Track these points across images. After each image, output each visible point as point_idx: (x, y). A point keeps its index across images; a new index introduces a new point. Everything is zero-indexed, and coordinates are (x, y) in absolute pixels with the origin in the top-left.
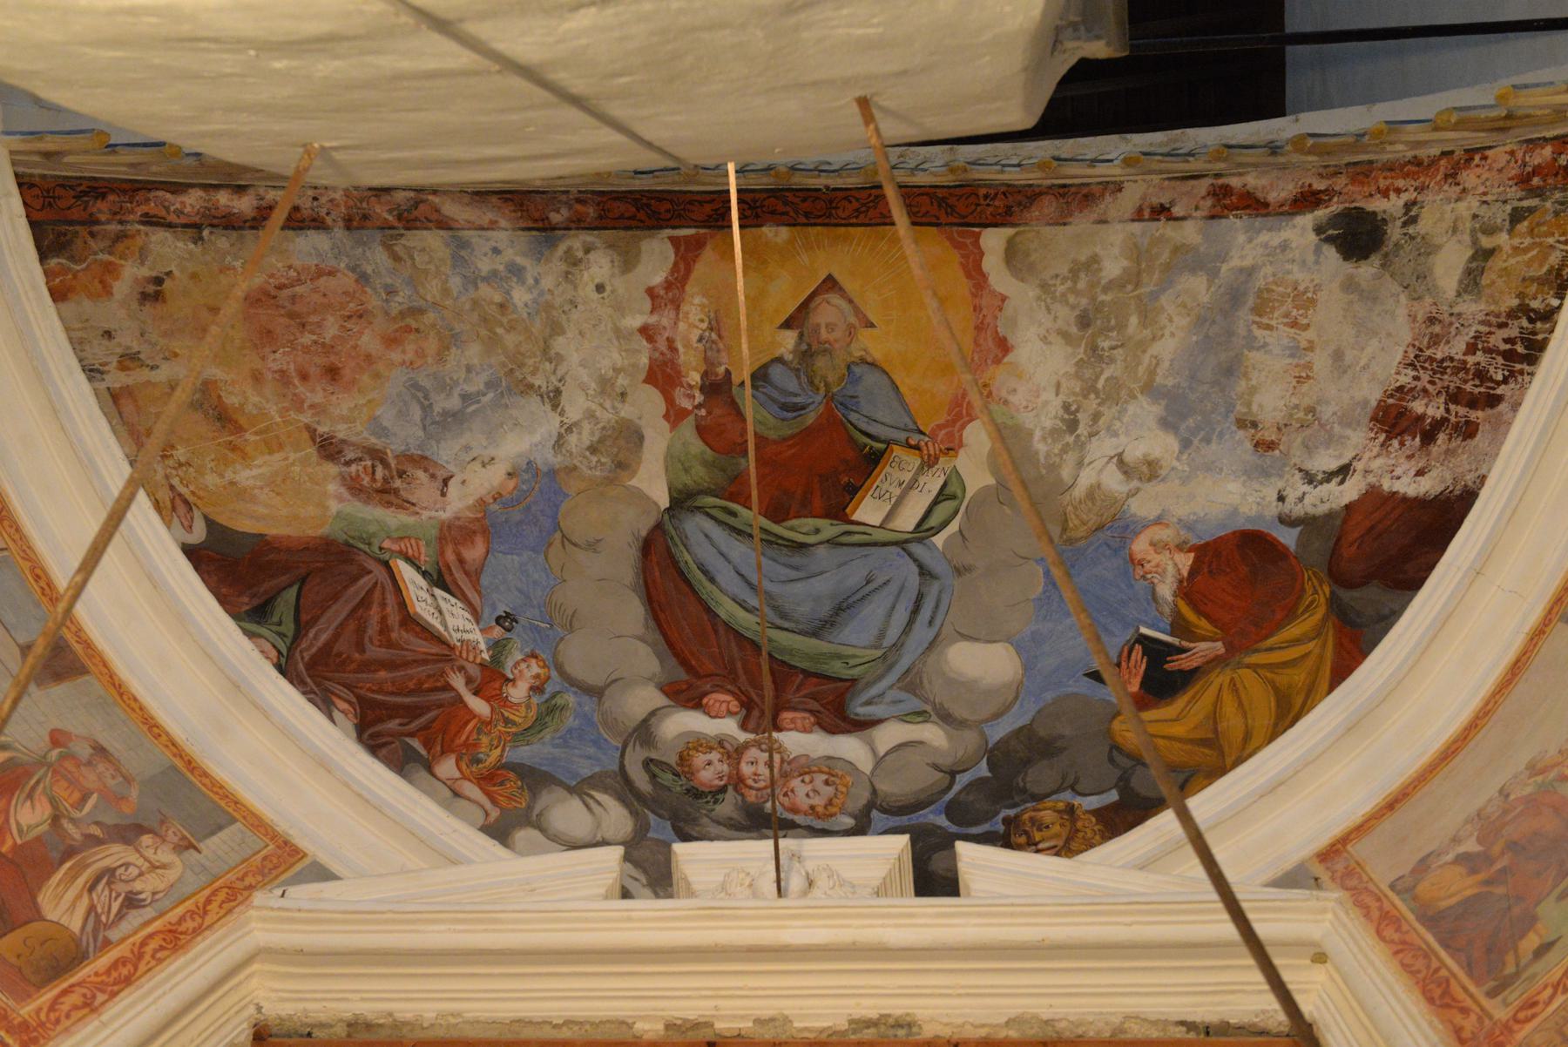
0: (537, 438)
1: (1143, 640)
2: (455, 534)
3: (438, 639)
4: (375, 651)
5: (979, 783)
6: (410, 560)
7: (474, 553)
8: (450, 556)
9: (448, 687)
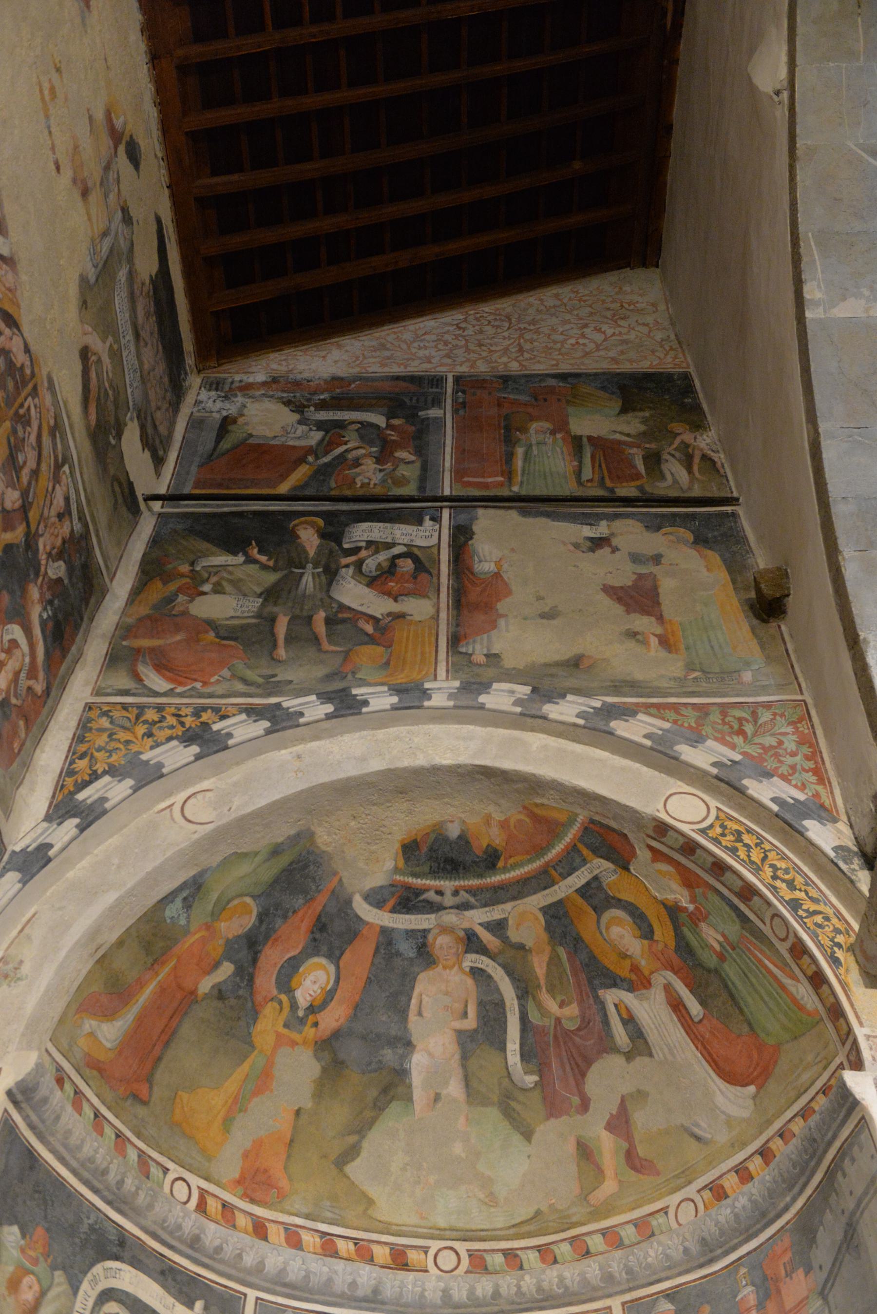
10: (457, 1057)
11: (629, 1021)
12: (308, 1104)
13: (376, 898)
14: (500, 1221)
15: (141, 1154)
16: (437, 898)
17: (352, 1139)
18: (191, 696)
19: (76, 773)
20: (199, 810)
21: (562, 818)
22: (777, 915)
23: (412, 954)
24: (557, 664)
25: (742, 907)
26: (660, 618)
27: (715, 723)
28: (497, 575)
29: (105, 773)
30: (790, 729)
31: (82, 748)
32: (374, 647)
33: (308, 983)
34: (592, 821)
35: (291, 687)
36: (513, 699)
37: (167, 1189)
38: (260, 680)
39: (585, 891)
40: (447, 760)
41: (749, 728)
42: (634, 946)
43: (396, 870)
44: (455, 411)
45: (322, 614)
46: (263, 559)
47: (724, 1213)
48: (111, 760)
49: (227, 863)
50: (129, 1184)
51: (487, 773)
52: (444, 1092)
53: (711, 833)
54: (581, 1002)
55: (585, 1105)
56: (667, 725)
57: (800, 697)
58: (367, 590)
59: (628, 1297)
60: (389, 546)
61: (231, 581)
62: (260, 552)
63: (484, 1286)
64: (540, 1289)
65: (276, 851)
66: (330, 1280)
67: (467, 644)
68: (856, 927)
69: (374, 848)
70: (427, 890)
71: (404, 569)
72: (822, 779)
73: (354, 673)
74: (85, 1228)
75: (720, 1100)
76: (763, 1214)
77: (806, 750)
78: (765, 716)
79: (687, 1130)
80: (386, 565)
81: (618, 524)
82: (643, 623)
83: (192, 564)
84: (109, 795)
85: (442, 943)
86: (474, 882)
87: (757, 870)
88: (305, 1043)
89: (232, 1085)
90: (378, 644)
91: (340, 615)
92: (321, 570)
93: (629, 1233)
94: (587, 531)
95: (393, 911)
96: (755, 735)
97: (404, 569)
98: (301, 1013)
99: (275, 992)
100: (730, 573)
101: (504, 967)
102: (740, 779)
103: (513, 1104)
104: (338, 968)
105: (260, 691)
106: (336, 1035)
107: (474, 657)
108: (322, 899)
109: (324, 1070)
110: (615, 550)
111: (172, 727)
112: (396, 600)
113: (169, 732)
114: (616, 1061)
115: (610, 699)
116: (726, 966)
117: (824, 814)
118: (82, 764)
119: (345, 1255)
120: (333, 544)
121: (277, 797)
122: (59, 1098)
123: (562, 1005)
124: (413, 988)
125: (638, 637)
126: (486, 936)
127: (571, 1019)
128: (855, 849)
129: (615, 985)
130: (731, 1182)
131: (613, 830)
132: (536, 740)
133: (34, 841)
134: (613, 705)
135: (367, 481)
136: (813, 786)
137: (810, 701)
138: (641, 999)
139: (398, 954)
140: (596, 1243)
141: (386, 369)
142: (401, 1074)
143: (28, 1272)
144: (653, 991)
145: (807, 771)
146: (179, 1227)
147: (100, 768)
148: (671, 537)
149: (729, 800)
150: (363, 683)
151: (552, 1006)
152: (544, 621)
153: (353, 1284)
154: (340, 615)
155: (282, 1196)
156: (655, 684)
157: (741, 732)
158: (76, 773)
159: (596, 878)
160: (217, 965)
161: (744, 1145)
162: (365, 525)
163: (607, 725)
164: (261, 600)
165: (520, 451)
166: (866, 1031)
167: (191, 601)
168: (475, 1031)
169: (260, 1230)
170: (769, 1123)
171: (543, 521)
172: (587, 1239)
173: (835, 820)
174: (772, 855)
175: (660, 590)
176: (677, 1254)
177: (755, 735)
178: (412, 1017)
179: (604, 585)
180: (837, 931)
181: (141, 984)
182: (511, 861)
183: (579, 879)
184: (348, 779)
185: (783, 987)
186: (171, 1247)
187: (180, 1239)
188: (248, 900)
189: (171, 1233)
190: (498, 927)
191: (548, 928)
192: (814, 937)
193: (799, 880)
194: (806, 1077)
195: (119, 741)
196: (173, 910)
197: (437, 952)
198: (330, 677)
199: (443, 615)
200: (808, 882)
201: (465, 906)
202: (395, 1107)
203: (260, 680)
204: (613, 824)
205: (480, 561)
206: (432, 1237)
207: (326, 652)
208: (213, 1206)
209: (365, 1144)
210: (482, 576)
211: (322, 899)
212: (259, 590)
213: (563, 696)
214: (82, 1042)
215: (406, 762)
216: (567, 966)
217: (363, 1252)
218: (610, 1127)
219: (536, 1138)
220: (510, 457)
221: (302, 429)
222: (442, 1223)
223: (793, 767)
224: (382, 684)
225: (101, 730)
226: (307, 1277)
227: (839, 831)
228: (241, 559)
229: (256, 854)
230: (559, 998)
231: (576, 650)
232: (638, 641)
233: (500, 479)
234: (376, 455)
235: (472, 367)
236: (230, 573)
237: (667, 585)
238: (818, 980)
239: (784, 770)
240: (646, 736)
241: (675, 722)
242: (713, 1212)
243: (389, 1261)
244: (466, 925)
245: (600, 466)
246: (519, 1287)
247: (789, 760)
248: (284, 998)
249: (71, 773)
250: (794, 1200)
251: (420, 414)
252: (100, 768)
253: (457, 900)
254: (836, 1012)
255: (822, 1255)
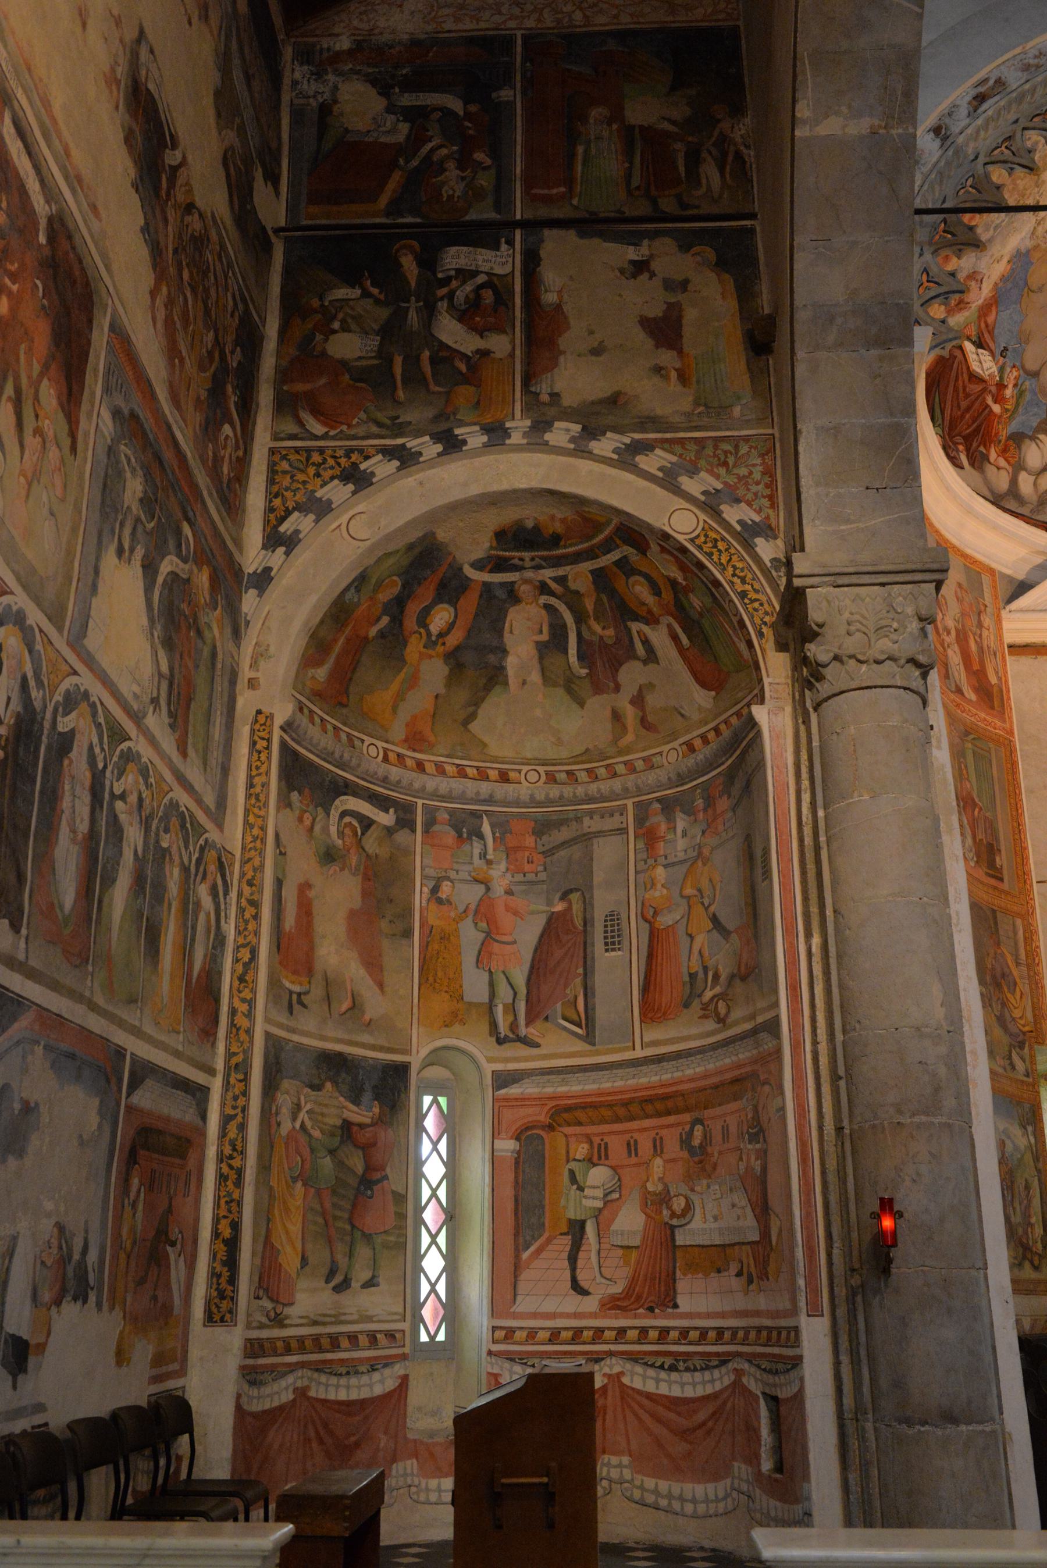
0: (1024, 234)
2: (984, 310)
3: (981, 380)
4: (964, 404)
6: (969, 338)
7: (990, 319)
8: (983, 325)
9: (987, 406)
10: (537, 657)
11: (646, 642)
12: (442, 691)
13: (479, 565)
14: (564, 754)
15: (348, 735)
16: (521, 563)
17: (471, 709)
18: (341, 439)
19: (275, 510)
20: (359, 529)
21: (602, 520)
22: (731, 601)
23: (504, 597)
24: (601, 402)
25: (713, 590)
26: (680, 352)
27: (709, 456)
28: (558, 307)
29: (294, 509)
30: (759, 461)
31: (275, 488)
32: (467, 387)
33: (437, 620)
34: (621, 524)
35: (411, 427)
36: (568, 437)
37: (365, 752)
38: (388, 422)
39: (618, 563)
40: (523, 486)
41: (731, 460)
42: (650, 599)
43: (491, 548)
44: (524, 93)
45: (426, 354)
46: (375, 291)
47: (691, 762)
48: (296, 498)
49: (379, 560)
50: (346, 756)
51: (552, 492)
52: (528, 679)
53: (697, 542)
54: (615, 628)
55: (617, 688)
56: (674, 459)
57: (770, 431)
58: (459, 326)
59: (637, 799)
60: (474, 274)
61: (353, 317)
62: (372, 285)
63: (554, 792)
64: (586, 795)
65: (410, 547)
66: (464, 792)
67: (536, 383)
68: (778, 608)
69: (476, 536)
70: (513, 558)
71: (487, 301)
72: (774, 505)
73: (455, 414)
74: (327, 783)
75: (696, 695)
76: (711, 765)
77: (767, 479)
78: (744, 449)
79: (676, 709)
80: (472, 296)
81: (657, 243)
82: (667, 358)
83: (321, 298)
84: (300, 528)
85: (524, 589)
86: (545, 553)
87: (723, 569)
88: (438, 656)
89: (395, 687)
90: (470, 384)
91: (441, 354)
92: (421, 304)
93: (640, 765)
94: (632, 253)
95: (491, 571)
96: (734, 466)
97: (487, 301)
98: (434, 638)
99: (416, 628)
100: (739, 302)
101: (566, 604)
102: (719, 505)
103: (573, 686)
104: (456, 609)
105: (388, 433)
106: (458, 648)
107: (541, 396)
108: (443, 569)
109: (451, 670)
110: (653, 275)
111: (332, 468)
112: (482, 337)
113: (330, 472)
114: (637, 665)
115: (637, 436)
116: (703, 621)
117: (769, 533)
118: (277, 502)
119: (471, 776)
120: (429, 273)
121: (410, 518)
122: (303, 721)
123: (604, 628)
124: (505, 617)
125: (663, 372)
126: (553, 585)
127: (609, 637)
128: (784, 560)
129: (638, 620)
130: (697, 743)
131: (636, 531)
132: (585, 466)
133: (260, 564)
134: (638, 441)
135: (451, 192)
136: (767, 510)
137: (777, 435)
138: (653, 630)
139: (495, 597)
140: (621, 769)
141: (461, 26)
142: (501, 669)
143: (306, 811)
144: (660, 626)
145: (764, 497)
146: (376, 773)
147: (290, 505)
148: (699, 259)
149: (712, 517)
150: (462, 424)
151: (597, 628)
152: (594, 358)
153: (478, 793)
154: (441, 354)
155: (431, 746)
156: (671, 419)
157: (725, 464)
158: (275, 510)
159: (625, 557)
160: (378, 619)
161: (706, 724)
162: (453, 250)
163: (633, 459)
164: (379, 338)
165: (580, 150)
166: (770, 680)
167: (326, 340)
168: (548, 642)
169: (420, 766)
170: (720, 714)
171: (596, 241)
172: (616, 767)
173: (775, 538)
174: (735, 558)
175: (684, 322)
176: (664, 779)
177: (734, 466)
178: (506, 634)
179: (641, 316)
180: (766, 613)
181: (335, 641)
182: (569, 542)
183: (614, 556)
184: (456, 501)
185: (734, 643)
186: (371, 783)
187: (377, 779)
188: (395, 578)
189: (372, 777)
190: (562, 580)
191: (594, 582)
192: (751, 617)
193: (750, 576)
194: (740, 695)
195: (298, 481)
196: (348, 596)
197: (521, 594)
198: (436, 419)
199: (518, 352)
200: (755, 578)
201: (539, 567)
202: (498, 689)
203: (388, 422)
204: (636, 528)
205: (546, 291)
206: (523, 764)
207: (433, 393)
208: (392, 757)
209: (480, 712)
210: (548, 309)
211: (443, 569)
212: (376, 327)
213: (604, 434)
214: (308, 683)
215: (496, 487)
216: (607, 605)
217: (483, 775)
218: (632, 702)
219: (587, 706)
220: (572, 156)
221: (391, 118)
222: (529, 755)
223: (756, 494)
224: (475, 424)
225: (285, 472)
226: (450, 791)
227: (778, 547)
228: (358, 292)
229: (398, 551)
230: (602, 624)
231: (616, 389)
232: (662, 376)
233: (562, 189)
234: (456, 156)
235: (539, 20)
236: (352, 309)
237: (690, 315)
238: (750, 644)
239: (750, 496)
240: (660, 469)
241: (681, 456)
242: (685, 760)
243: (498, 778)
244: (540, 578)
245: (648, 168)
246: (575, 793)
247: (754, 488)
248: (422, 630)
249: (271, 510)
250: (727, 760)
251: (494, 95)
252: (290, 505)
253: (533, 563)
254: (757, 667)
255: (736, 789)
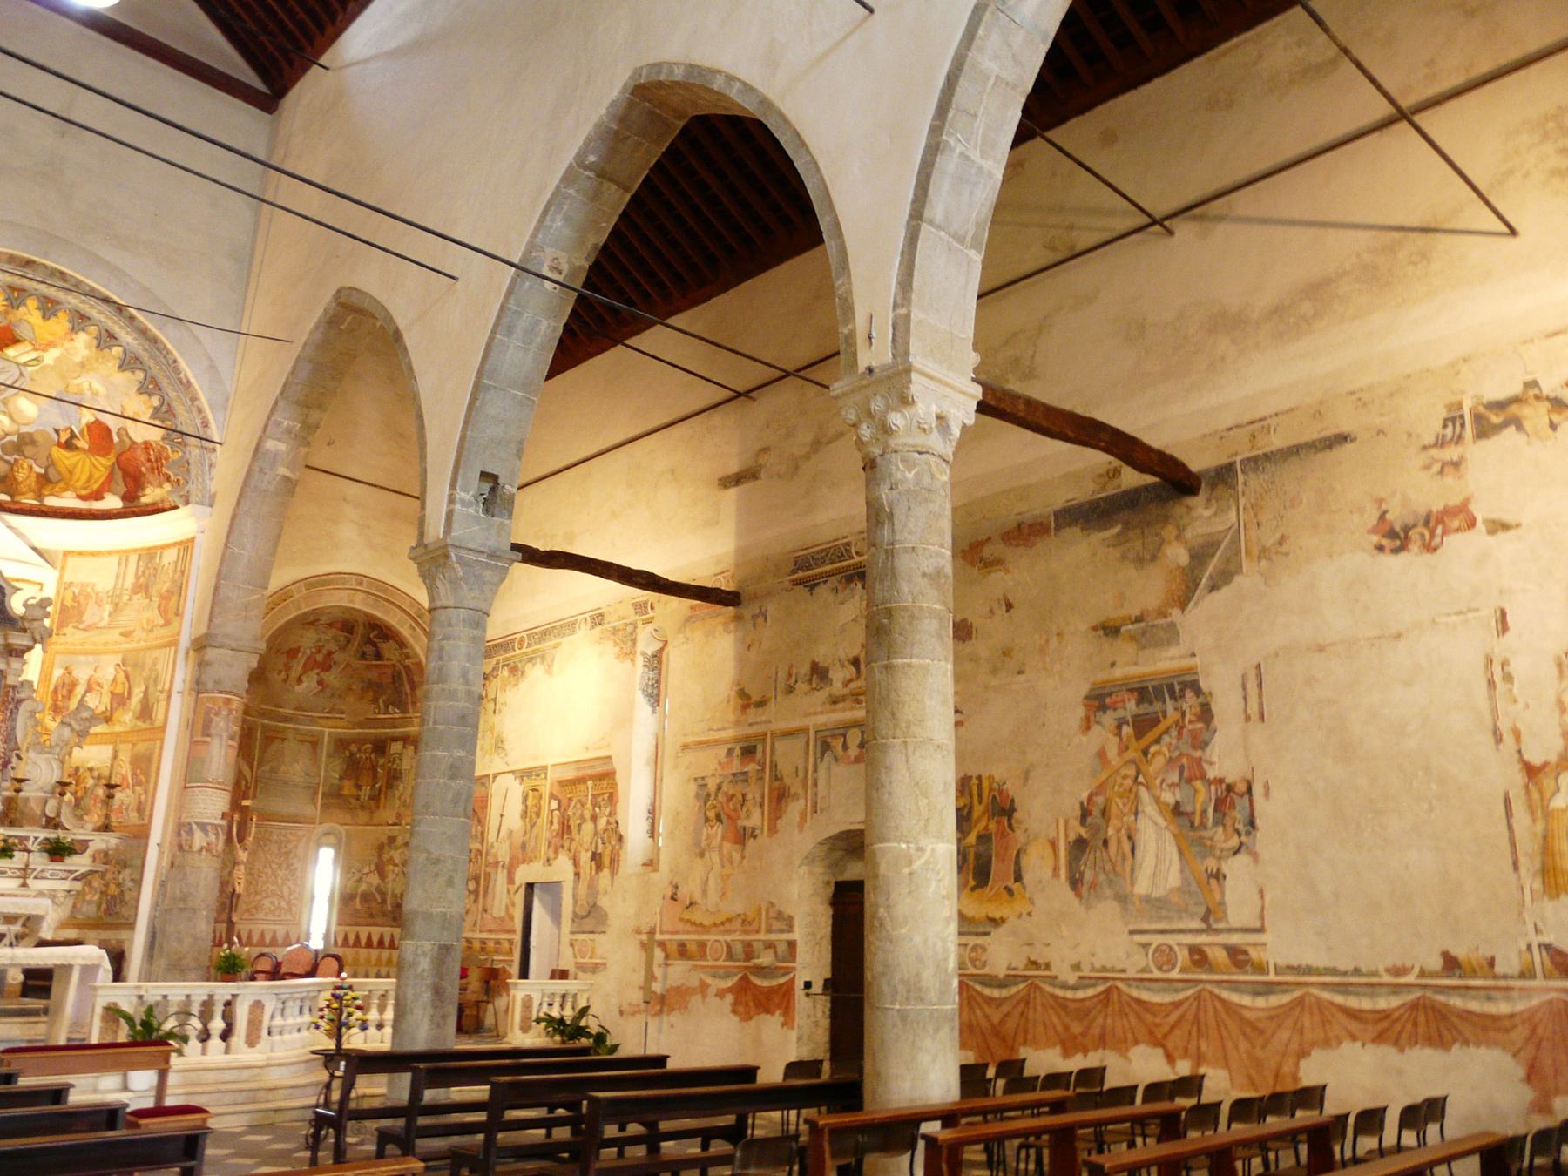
1: (72, 431)
5: (12, 442)
